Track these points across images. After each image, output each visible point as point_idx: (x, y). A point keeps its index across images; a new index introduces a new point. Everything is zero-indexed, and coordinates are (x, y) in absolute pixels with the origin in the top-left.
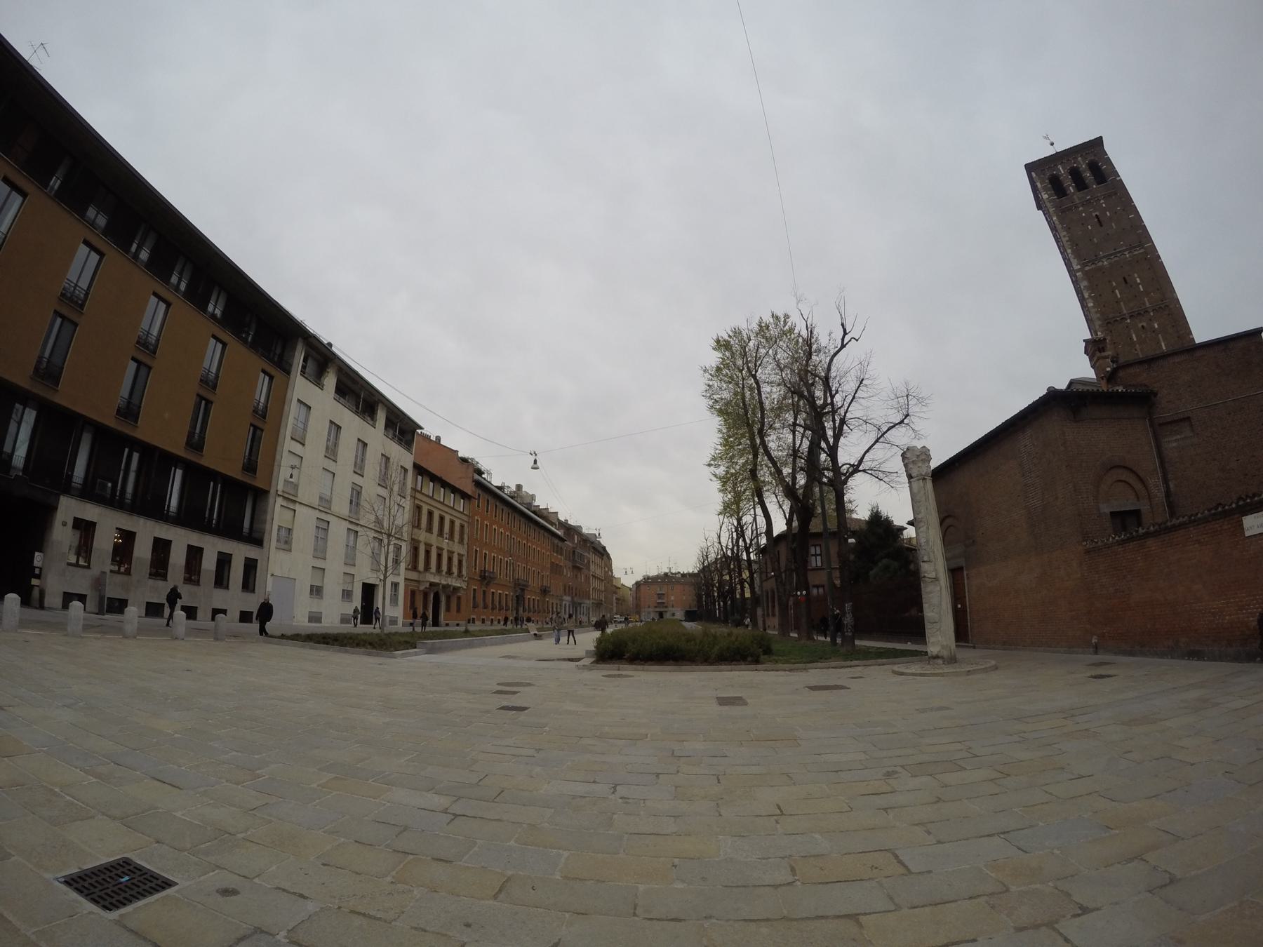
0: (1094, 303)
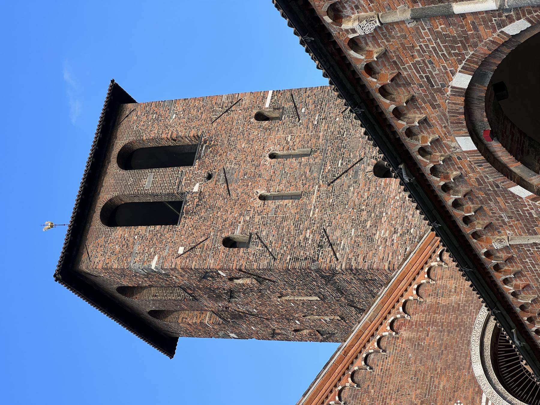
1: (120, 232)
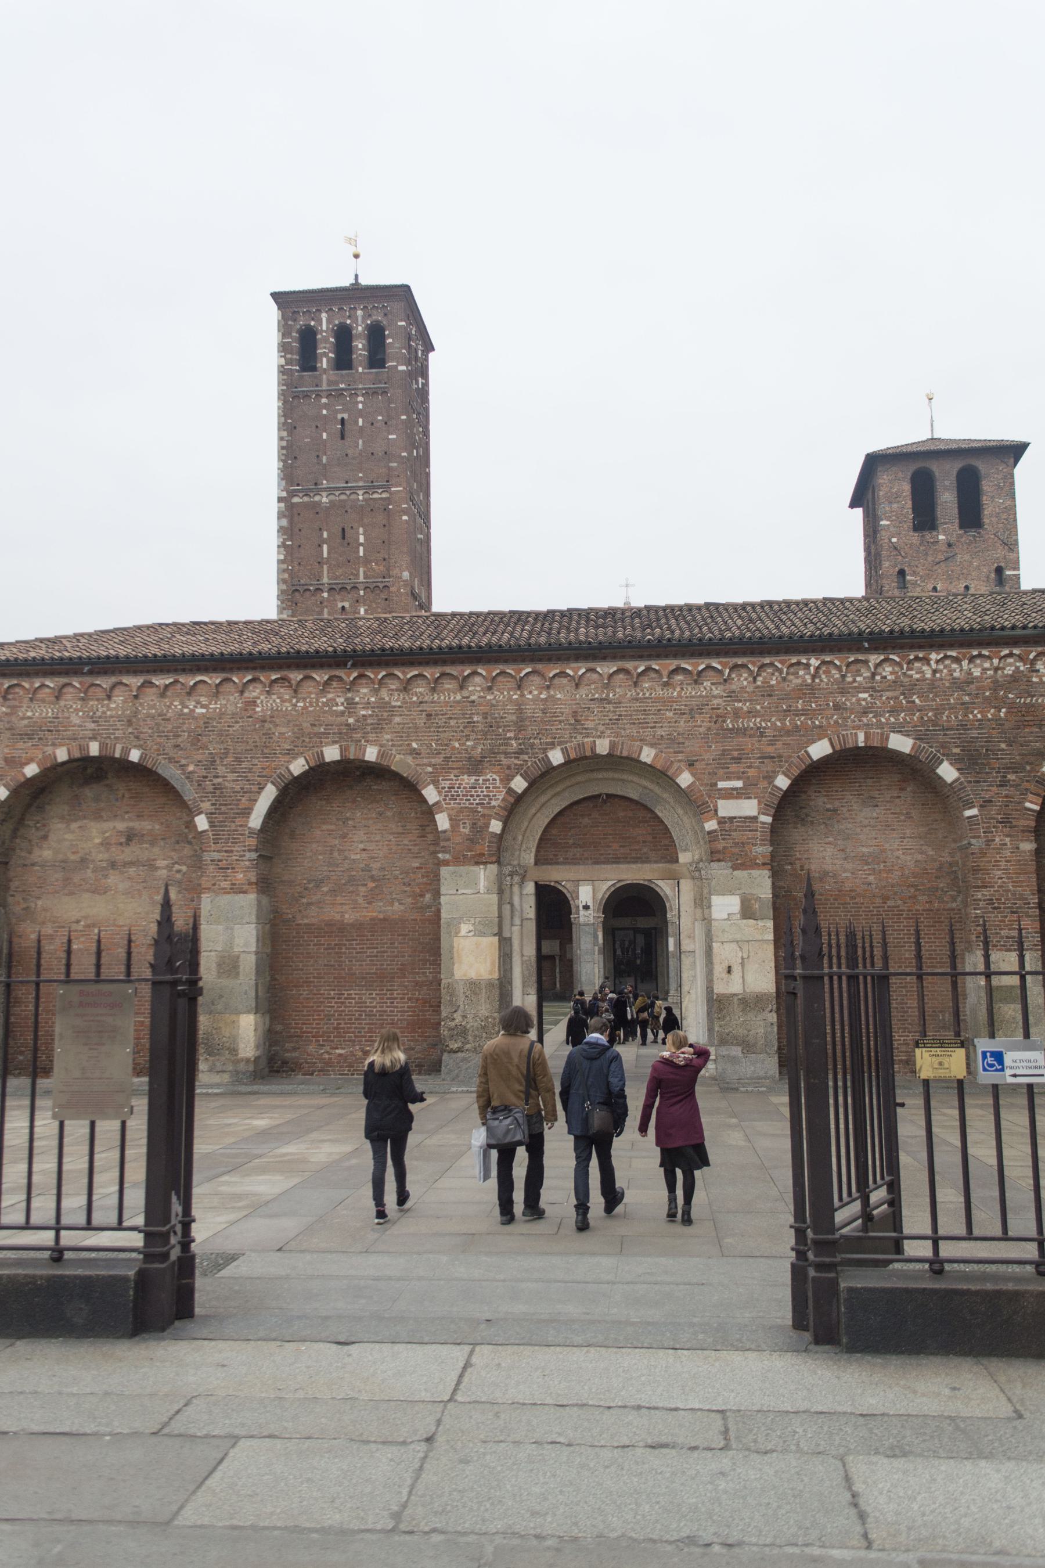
0: (285, 556)
1: (907, 487)
